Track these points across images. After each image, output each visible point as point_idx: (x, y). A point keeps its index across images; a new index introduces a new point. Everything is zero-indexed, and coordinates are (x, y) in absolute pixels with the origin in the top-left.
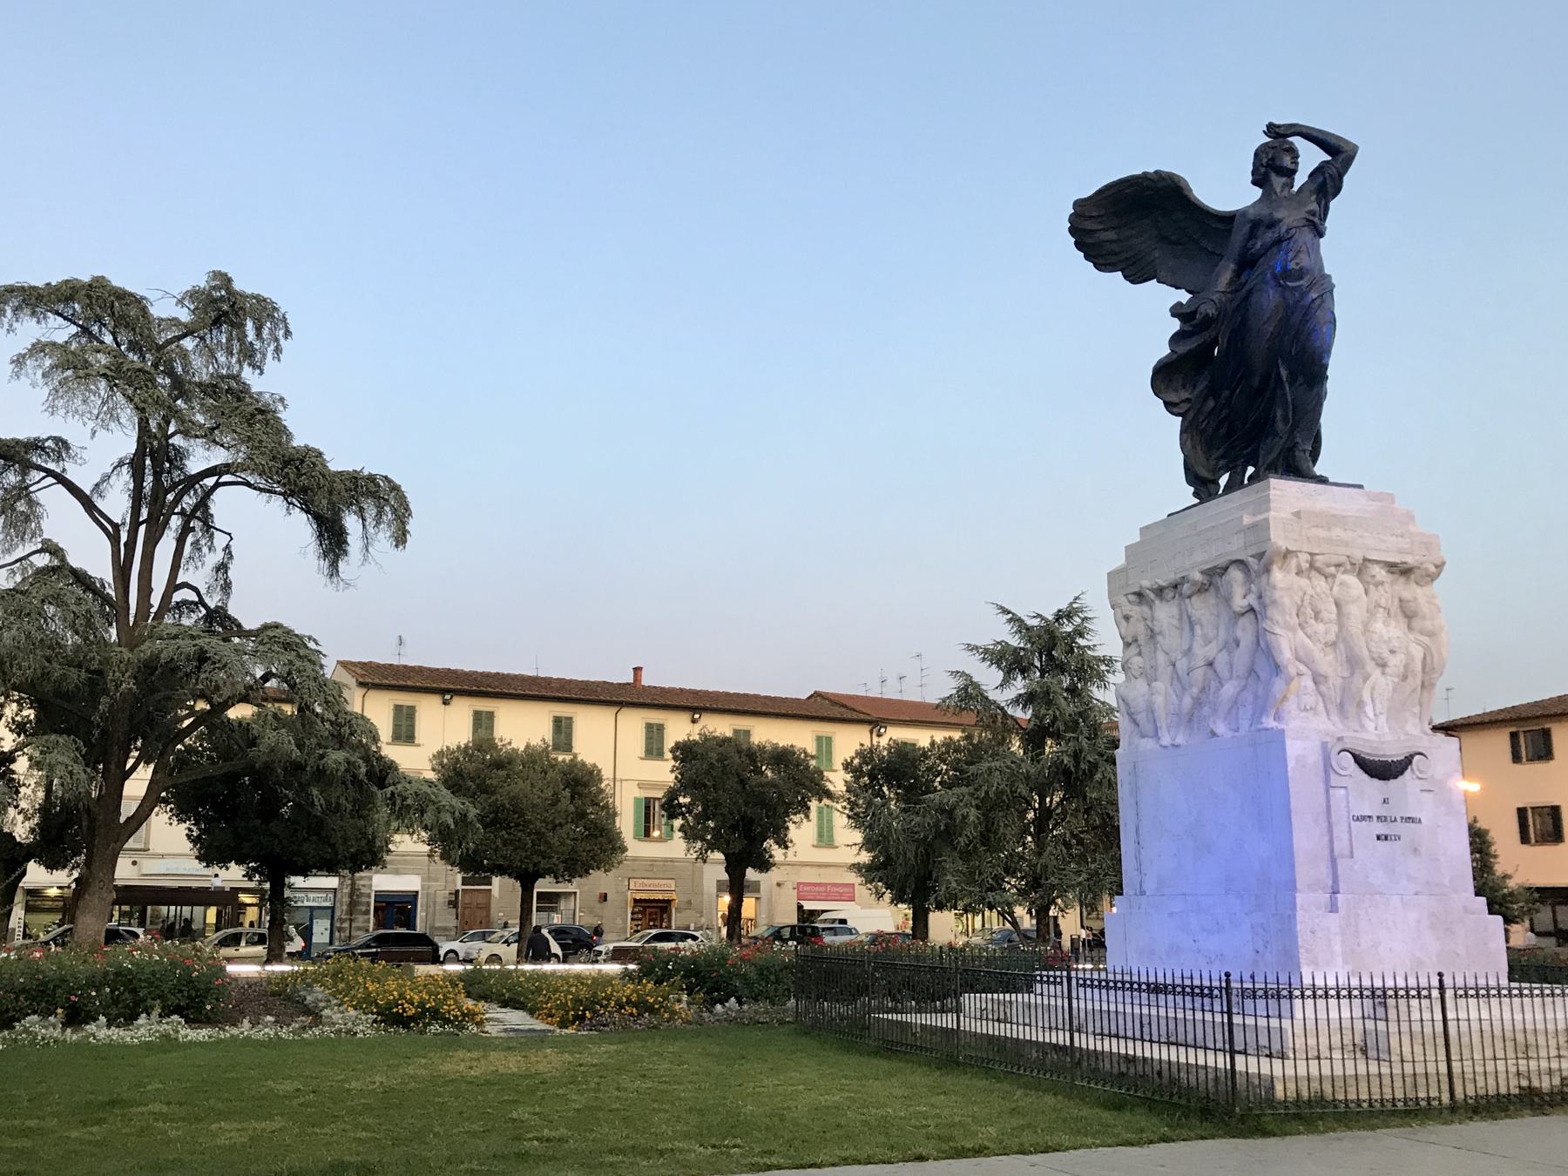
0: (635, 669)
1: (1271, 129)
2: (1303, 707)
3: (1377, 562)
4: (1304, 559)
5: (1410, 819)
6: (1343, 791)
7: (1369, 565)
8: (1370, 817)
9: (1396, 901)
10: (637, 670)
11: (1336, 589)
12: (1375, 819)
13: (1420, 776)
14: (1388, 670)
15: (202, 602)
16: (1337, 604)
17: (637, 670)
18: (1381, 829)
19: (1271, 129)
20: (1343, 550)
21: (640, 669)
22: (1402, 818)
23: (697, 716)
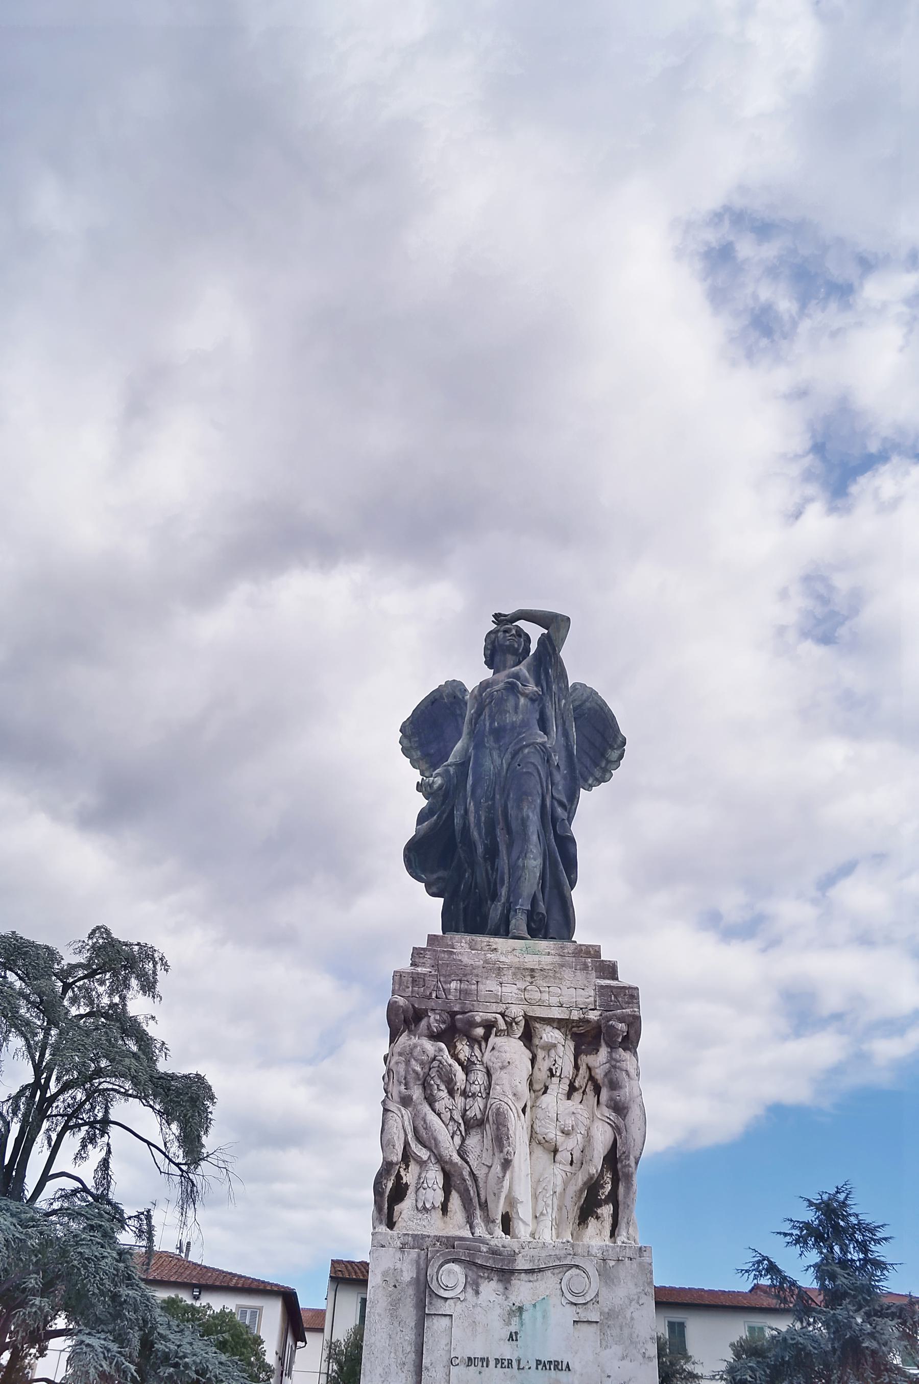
1: (498, 618)
2: (420, 1205)
3: (548, 1021)
4: (434, 1021)
5: (557, 1365)
6: (445, 1321)
7: (537, 1025)
8: (482, 1359)
11: (487, 1055)
12: (492, 1363)
13: (574, 1300)
14: (558, 1157)
15: (85, 1189)
16: (489, 1074)
19: (498, 618)
20: (494, 1007)
22: (538, 1362)
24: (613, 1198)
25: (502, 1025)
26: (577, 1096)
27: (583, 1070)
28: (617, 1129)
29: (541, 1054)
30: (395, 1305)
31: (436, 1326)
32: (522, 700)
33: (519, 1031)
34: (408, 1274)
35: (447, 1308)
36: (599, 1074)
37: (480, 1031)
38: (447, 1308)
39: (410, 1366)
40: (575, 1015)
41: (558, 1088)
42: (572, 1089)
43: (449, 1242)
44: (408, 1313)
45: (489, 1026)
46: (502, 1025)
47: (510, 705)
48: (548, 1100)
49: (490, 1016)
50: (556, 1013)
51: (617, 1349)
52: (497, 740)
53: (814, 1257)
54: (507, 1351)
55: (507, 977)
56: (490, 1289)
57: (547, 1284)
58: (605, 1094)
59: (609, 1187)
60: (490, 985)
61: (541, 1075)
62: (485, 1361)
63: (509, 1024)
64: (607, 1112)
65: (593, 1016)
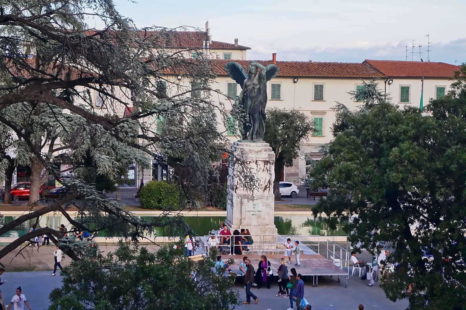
0: (273, 54)
5: (260, 211)
9: (253, 226)
10: (274, 55)
17: (274, 55)
18: (252, 213)
21: (276, 54)
23: (296, 80)
24: (269, 187)
25: (252, 162)
26: (264, 171)
27: (265, 168)
28: (270, 177)
29: (258, 165)
30: (237, 205)
31: (243, 207)
32: (256, 90)
33: (255, 162)
34: (239, 200)
35: (245, 205)
36: (268, 169)
37: (248, 163)
38: (245, 205)
39: (240, 212)
40: (264, 159)
41: (261, 171)
42: (263, 170)
43: (245, 195)
44: (239, 205)
45: (250, 162)
46: (252, 162)
47: (253, 92)
48: (259, 173)
49: (250, 161)
50: (262, 159)
51: (269, 209)
52: (251, 99)
53: (362, 104)
54: (253, 210)
55: (253, 153)
56: (251, 202)
57: (259, 201)
58: (268, 171)
59: (268, 186)
60: (250, 155)
61: (258, 168)
62: (250, 211)
63: (253, 162)
64: (269, 175)
65: (267, 160)
